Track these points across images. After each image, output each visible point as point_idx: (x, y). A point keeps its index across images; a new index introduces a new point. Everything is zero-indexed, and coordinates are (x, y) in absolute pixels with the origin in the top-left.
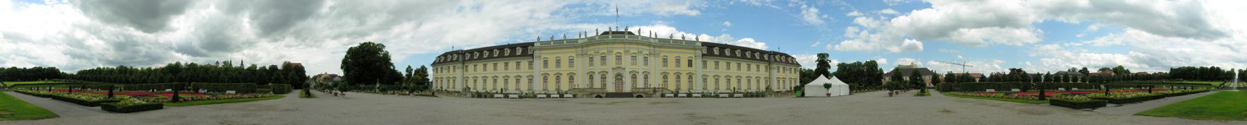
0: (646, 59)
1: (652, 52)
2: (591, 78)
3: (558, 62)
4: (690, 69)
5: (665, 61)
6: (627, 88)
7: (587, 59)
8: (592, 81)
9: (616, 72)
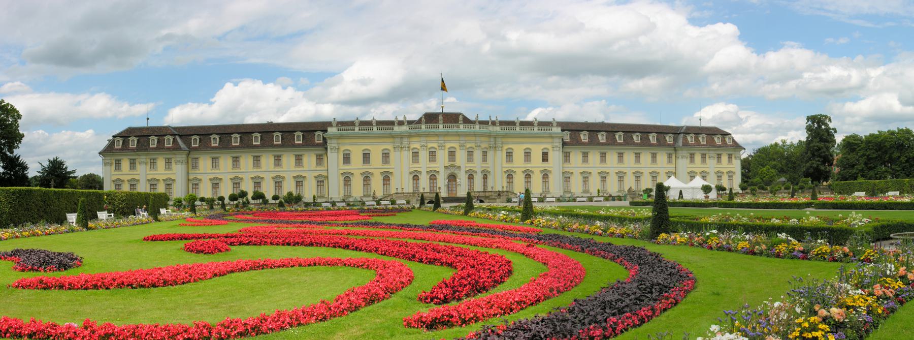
0: (485, 154)
1: (492, 144)
2: (416, 178)
3: (366, 157)
4: (545, 164)
5: (510, 155)
8: (417, 184)
9: (449, 172)
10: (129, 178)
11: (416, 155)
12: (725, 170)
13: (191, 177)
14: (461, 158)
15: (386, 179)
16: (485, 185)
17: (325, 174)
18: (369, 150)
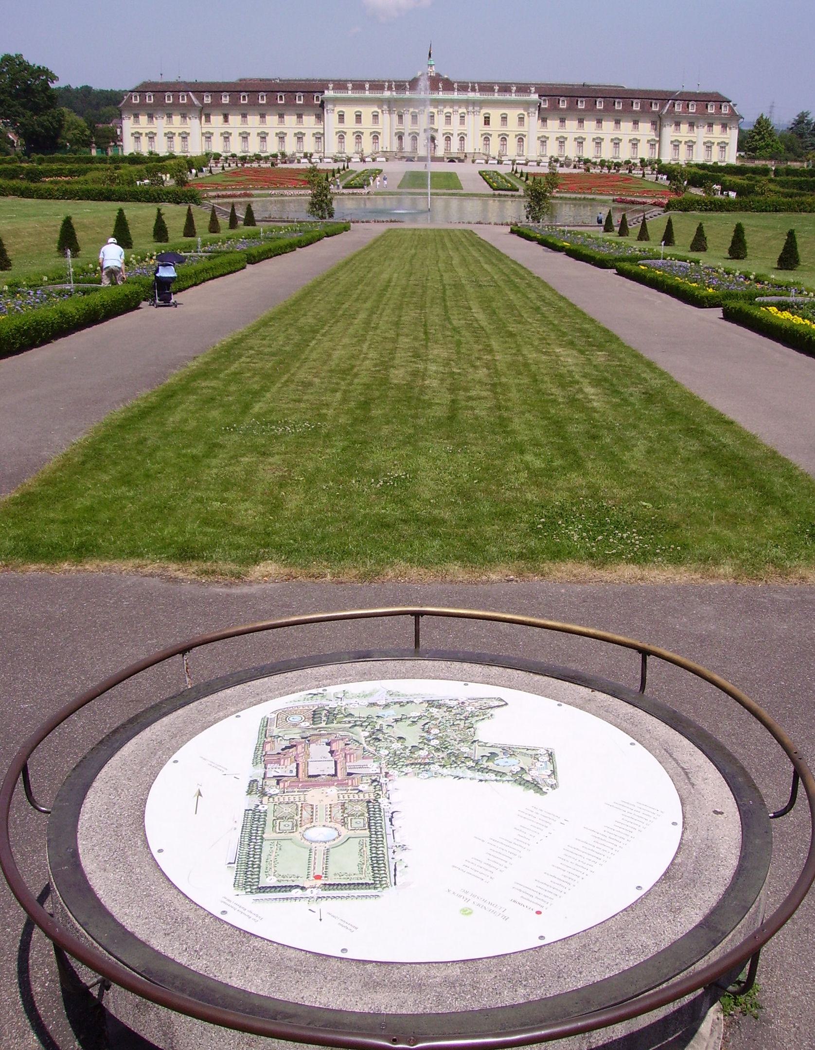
2: (400, 138)
3: (358, 117)
6: (440, 152)
7: (395, 117)
10: (147, 131)
11: (400, 117)
12: (683, 140)
14: (440, 121)
15: (376, 137)
16: (462, 146)
17: (322, 132)
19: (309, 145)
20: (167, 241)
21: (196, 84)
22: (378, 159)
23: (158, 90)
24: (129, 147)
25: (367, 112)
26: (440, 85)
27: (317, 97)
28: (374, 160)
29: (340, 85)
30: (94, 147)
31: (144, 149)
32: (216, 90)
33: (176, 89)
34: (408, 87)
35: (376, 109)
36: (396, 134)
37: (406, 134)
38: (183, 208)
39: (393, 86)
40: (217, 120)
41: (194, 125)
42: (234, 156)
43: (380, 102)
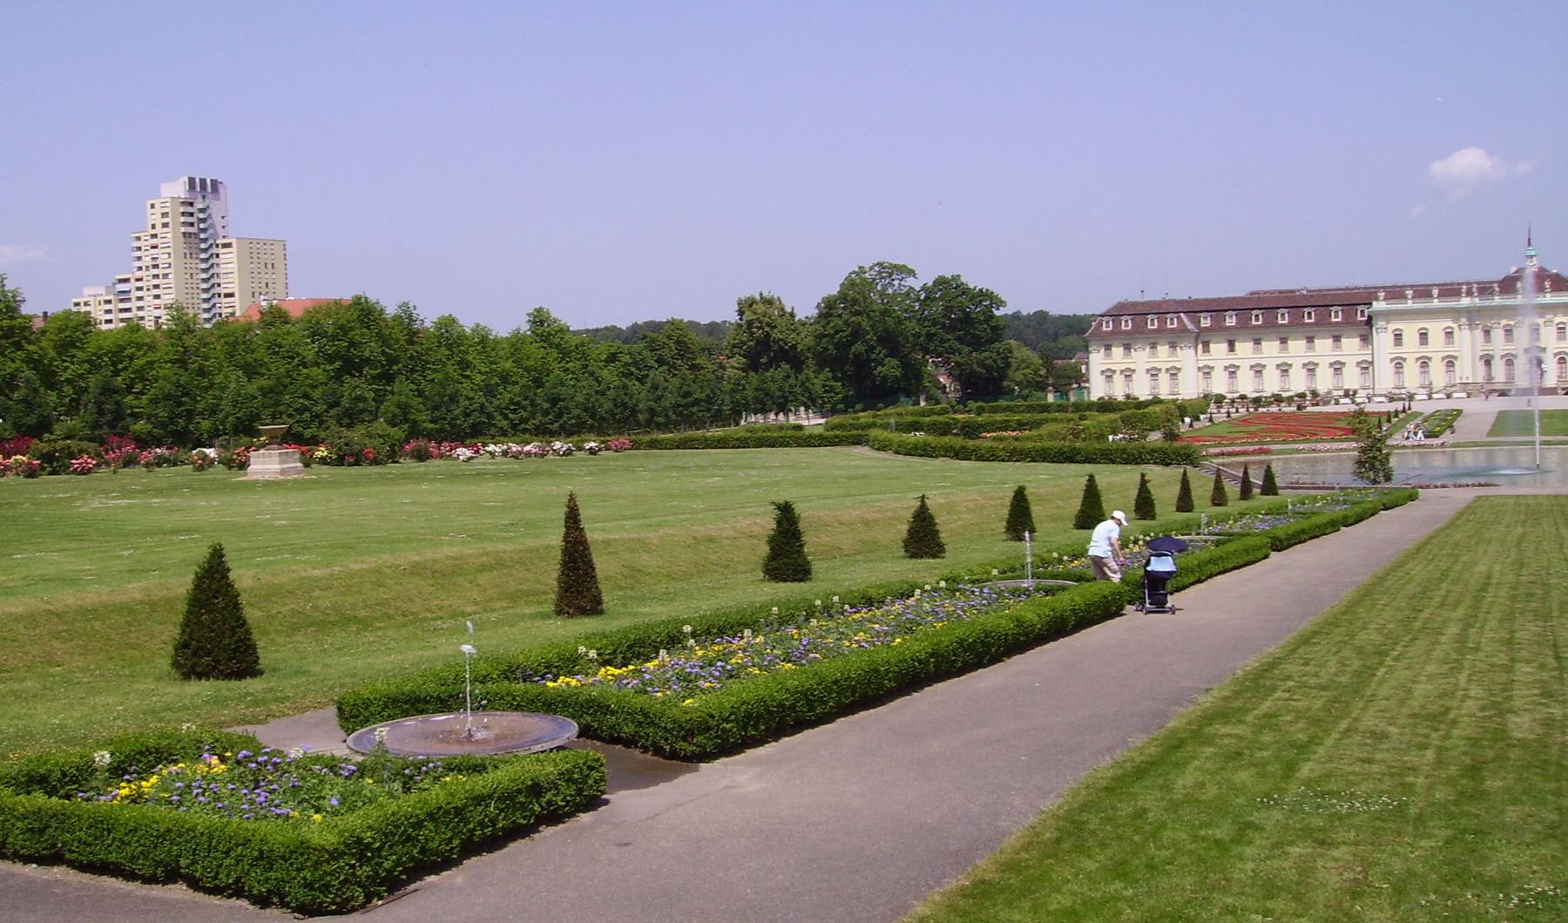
2: (1488, 363)
3: (1424, 337)
7: (1479, 334)
11: (1487, 333)
13: (1201, 365)
15: (1450, 363)
17: (1370, 360)
18: (1426, 329)
19: (1352, 379)
20: (1153, 518)
21: (1189, 301)
22: (1455, 395)
23: (1138, 312)
24: (1097, 390)
25: (1436, 328)
26: (1547, 284)
27: (1362, 311)
28: (1449, 396)
29: (1395, 293)
30: (1051, 391)
31: (1119, 392)
32: (1217, 308)
33: (1162, 309)
34: (1497, 289)
35: (1450, 324)
36: (1481, 357)
37: (1497, 358)
38: (1175, 472)
39: (1474, 290)
40: (1219, 349)
41: (1187, 357)
42: (1243, 397)
43: (1456, 313)
